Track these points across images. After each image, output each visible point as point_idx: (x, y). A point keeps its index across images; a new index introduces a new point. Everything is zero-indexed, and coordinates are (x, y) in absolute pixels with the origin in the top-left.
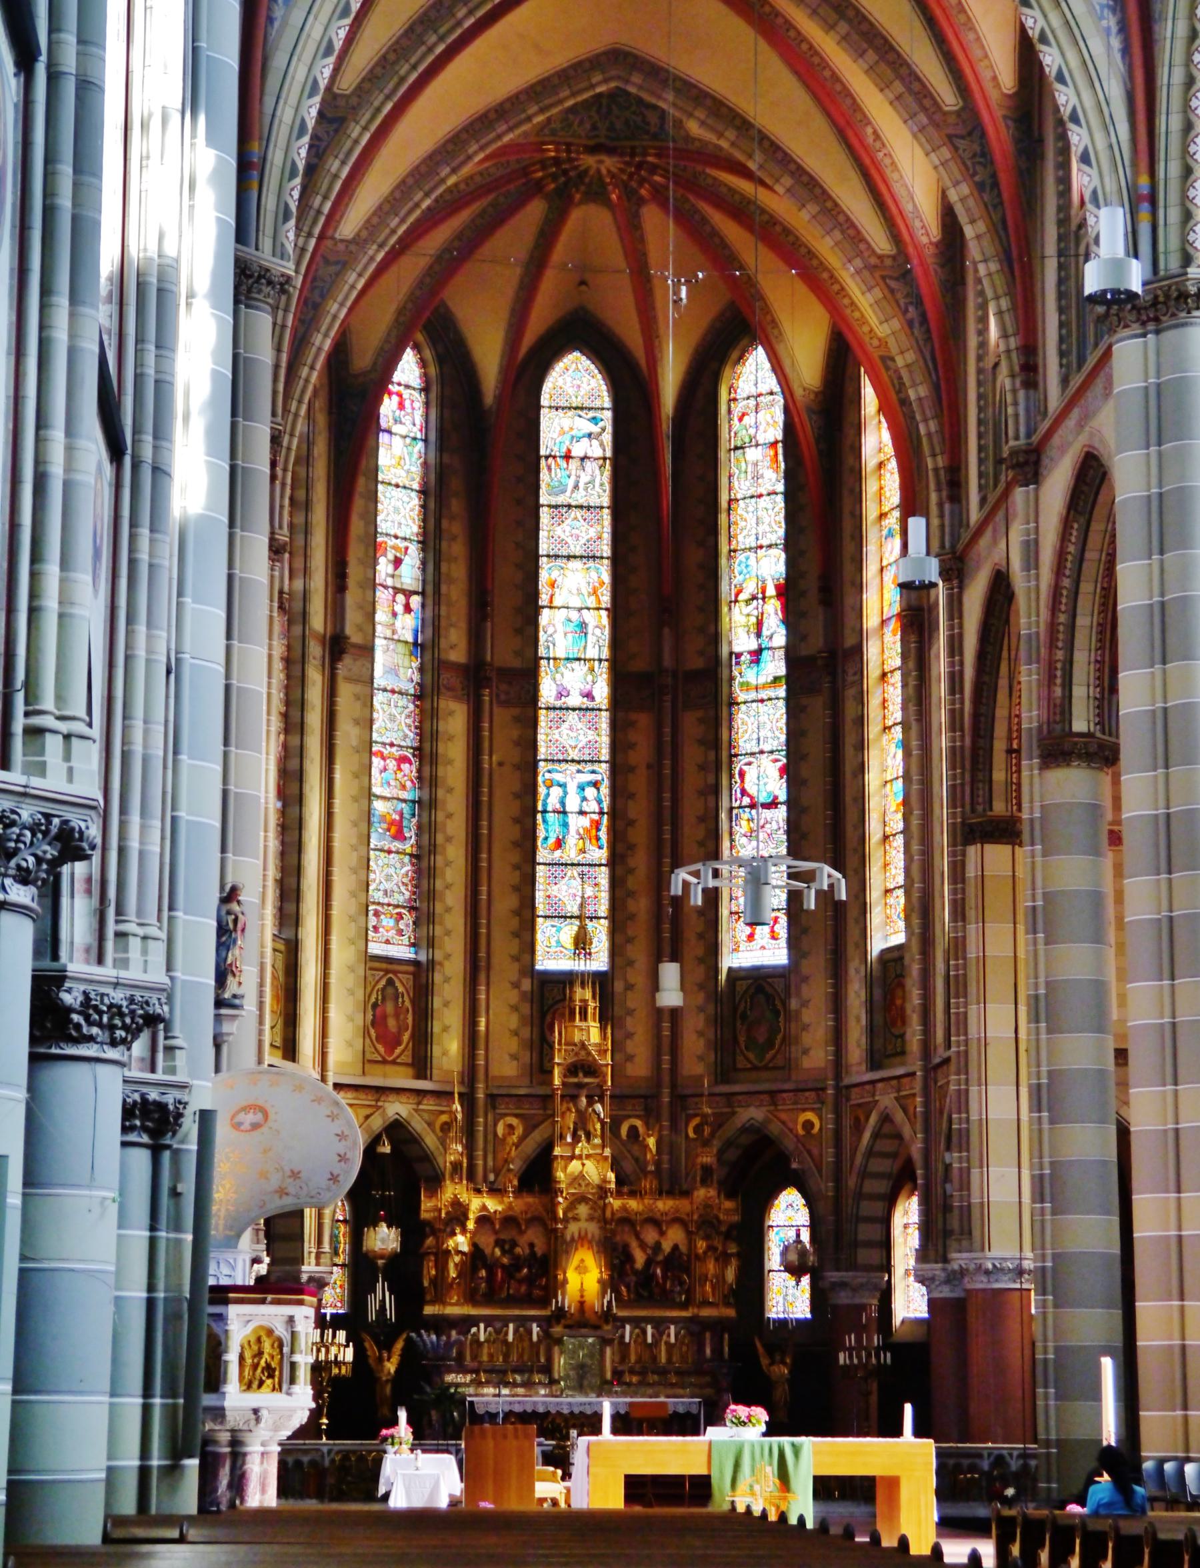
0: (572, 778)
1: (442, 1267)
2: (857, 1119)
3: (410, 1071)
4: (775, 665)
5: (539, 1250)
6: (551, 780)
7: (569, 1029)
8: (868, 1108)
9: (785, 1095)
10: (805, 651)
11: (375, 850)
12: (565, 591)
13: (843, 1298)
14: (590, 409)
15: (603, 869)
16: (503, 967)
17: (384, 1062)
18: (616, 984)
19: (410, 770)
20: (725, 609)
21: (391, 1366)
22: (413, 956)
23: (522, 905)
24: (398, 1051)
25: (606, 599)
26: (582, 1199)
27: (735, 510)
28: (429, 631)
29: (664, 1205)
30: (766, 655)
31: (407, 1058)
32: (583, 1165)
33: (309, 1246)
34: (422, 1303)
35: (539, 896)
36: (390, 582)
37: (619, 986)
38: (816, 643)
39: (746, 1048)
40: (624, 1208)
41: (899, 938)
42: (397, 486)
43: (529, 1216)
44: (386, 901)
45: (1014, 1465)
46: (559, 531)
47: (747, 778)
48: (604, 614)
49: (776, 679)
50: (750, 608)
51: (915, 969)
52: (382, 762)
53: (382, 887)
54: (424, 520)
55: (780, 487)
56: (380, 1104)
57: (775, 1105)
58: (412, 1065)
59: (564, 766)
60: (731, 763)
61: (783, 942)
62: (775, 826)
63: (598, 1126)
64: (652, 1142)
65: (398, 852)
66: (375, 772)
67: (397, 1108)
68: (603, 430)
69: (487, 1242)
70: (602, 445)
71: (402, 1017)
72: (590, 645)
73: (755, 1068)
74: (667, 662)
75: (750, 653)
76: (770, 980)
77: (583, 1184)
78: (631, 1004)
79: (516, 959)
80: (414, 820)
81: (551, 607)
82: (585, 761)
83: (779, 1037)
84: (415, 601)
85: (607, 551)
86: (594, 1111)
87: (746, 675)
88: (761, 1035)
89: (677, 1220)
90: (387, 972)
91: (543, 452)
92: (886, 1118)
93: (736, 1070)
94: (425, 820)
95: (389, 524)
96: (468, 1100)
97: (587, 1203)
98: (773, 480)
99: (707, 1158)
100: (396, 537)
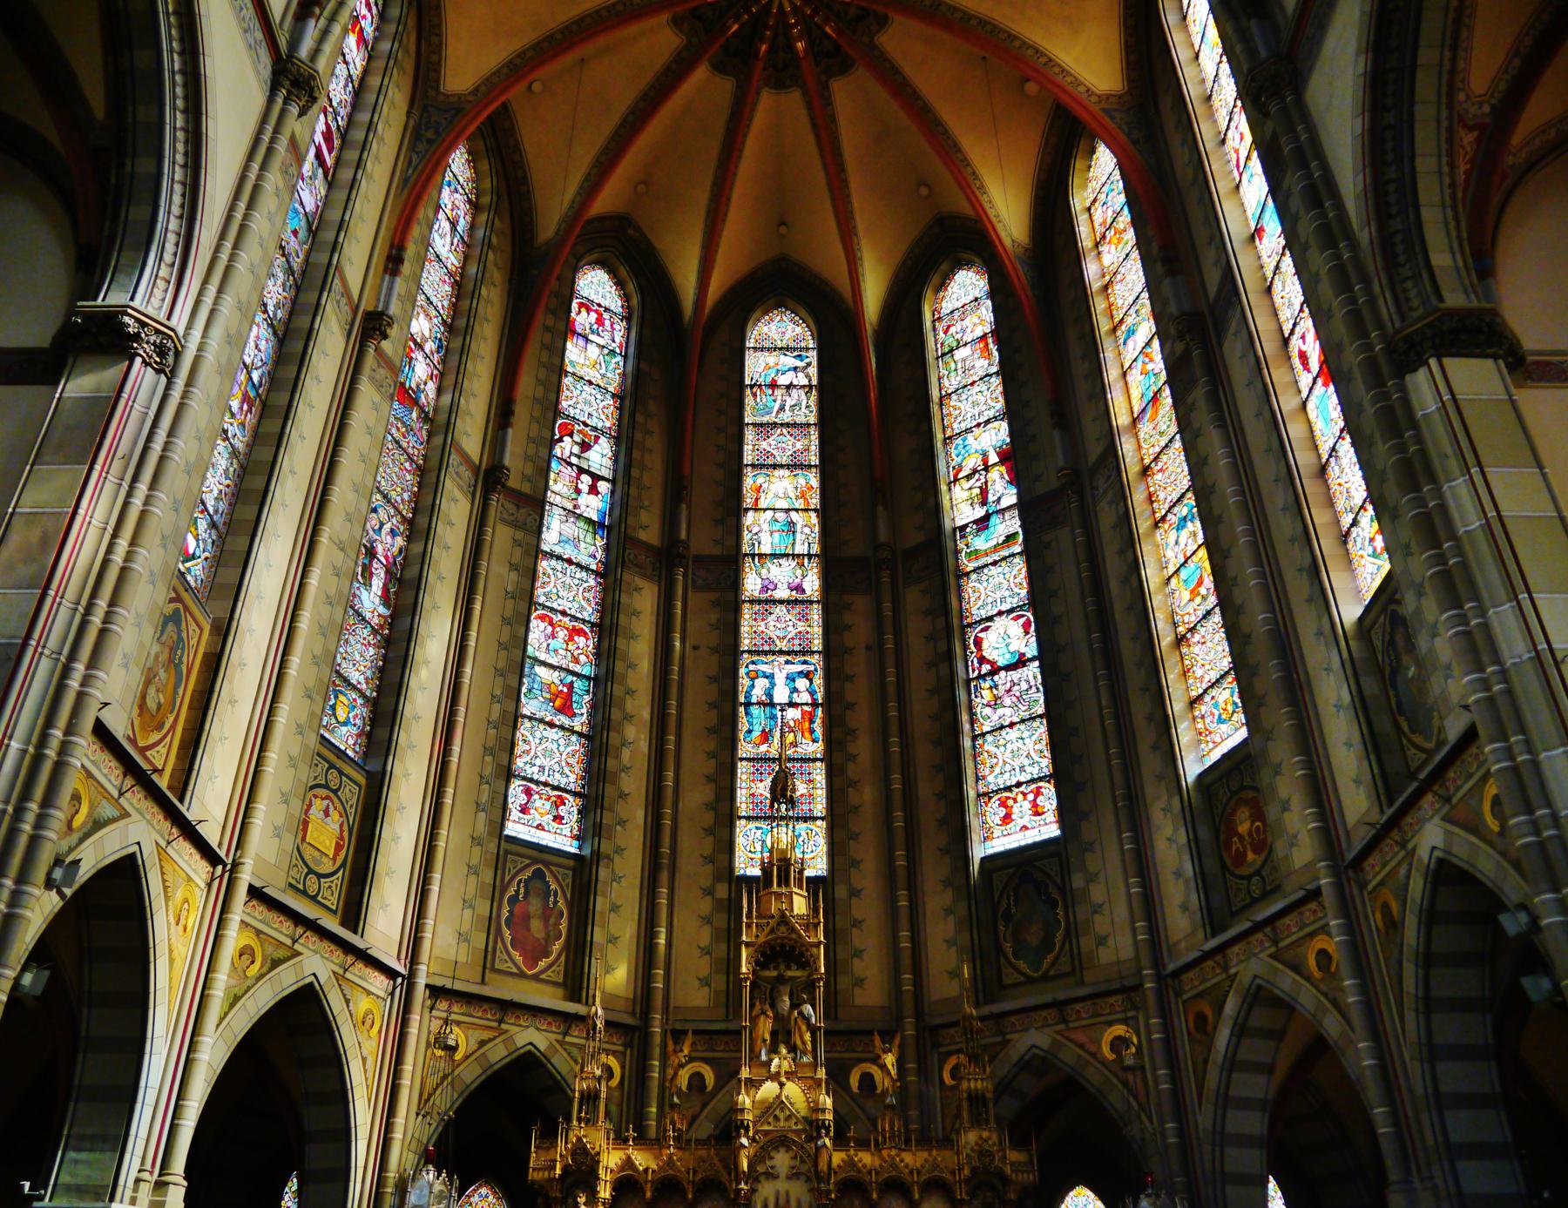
0: (781, 670)
2: (1201, 1018)
3: (560, 992)
6: (756, 672)
7: (763, 899)
9: (1078, 1006)
11: (530, 719)
12: (770, 495)
14: (795, 349)
15: (818, 764)
17: (522, 975)
18: (837, 888)
20: (944, 488)
22: (577, 851)
23: (718, 798)
24: (542, 964)
25: (815, 501)
26: (781, 1141)
27: (948, 404)
28: (617, 512)
29: (912, 1159)
30: (994, 520)
32: (782, 1085)
35: (741, 795)
36: (574, 460)
37: (841, 892)
38: (1056, 459)
40: (850, 1163)
42: (590, 383)
43: (699, 1177)
44: (543, 779)
46: (764, 445)
47: (985, 645)
48: (813, 515)
49: (1010, 538)
50: (973, 480)
52: (550, 629)
53: (538, 762)
54: (619, 420)
57: (1066, 1022)
58: (564, 985)
59: (771, 658)
60: (964, 634)
61: (1051, 817)
62: (1024, 686)
63: (808, 1036)
65: (562, 727)
67: (531, 1036)
68: (809, 365)
70: (807, 376)
71: (552, 920)
72: (798, 542)
73: (1030, 981)
74: (883, 535)
75: (975, 522)
76: (1038, 864)
77: (782, 1116)
78: (857, 913)
79: (709, 860)
80: (587, 698)
81: (756, 510)
82: (796, 653)
83: (1059, 935)
84: (603, 487)
85: (815, 460)
86: (801, 1013)
88: (1033, 937)
90: (535, 861)
91: (747, 382)
94: (600, 695)
95: (578, 411)
97: (788, 1149)
100: (586, 425)
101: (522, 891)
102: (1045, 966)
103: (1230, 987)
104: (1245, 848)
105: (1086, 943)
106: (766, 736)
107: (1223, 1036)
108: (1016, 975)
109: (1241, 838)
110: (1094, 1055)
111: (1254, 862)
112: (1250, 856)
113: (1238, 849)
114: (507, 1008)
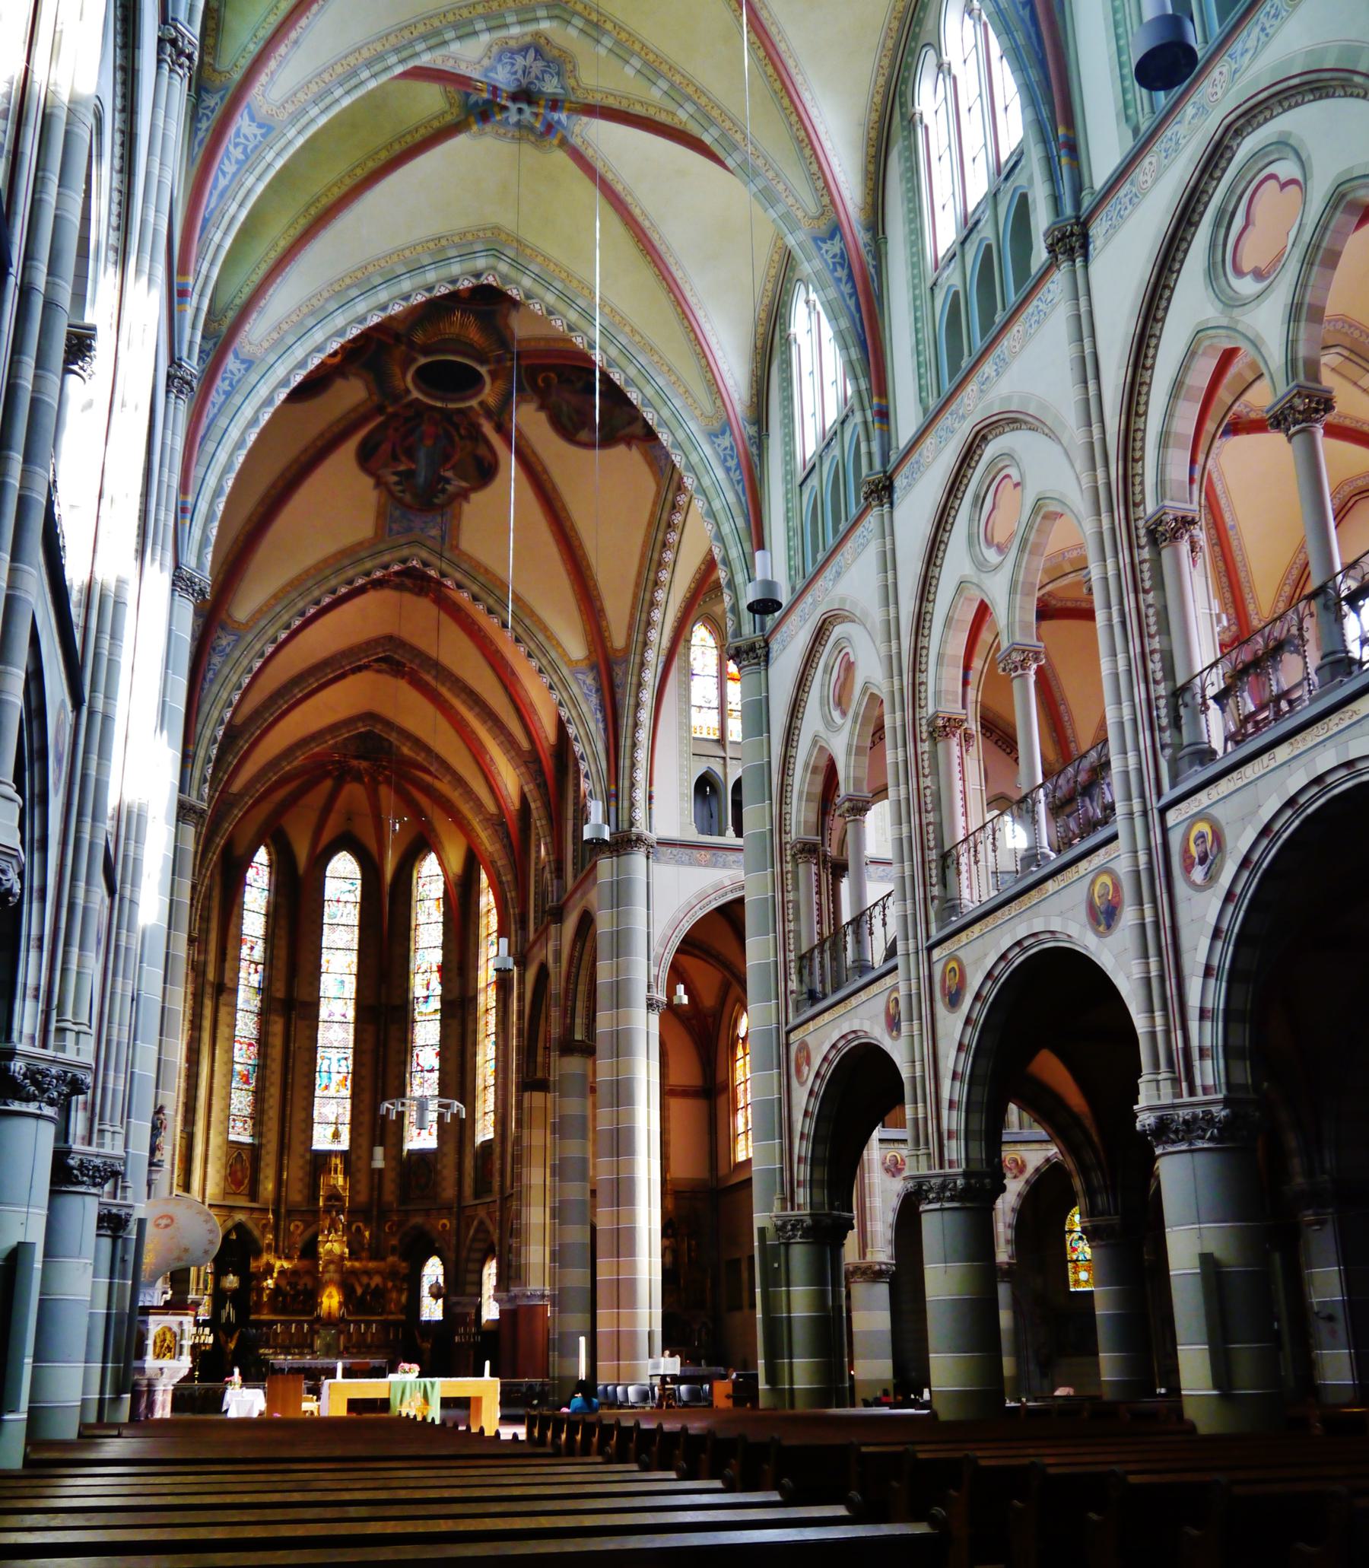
0: (334, 1055)
1: (260, 1296)
4: (435, 1004)
5: (309, 1287)
8: (472, 1218)
10: (450, 997)
13: (458, 1310)
16: (297, 1148)
19: (254, 1050)
21: (232, 1346)
25: (354, 969)
29: (372, 1265)
31: (246, 1192)
33: (193, 1285)
34: (250, 1313)
37: (353, 1157)
38: (455, 994)
41: (490, 1136)
45: (538, 1389)
51: (497, 1150)
55: (441, 919)
64: (367, 1234)
66: (236, 1050)
67: (240, 1217)
69: (283, 1283)
87: (420, 1008)
89: (378, 1272)
92: (481, 1223)
96: (276, 1213)
98: (438, 916)
99: (394, 1242)
106: (327, 1087)
107: (472, 1232)
114: (232, 1208)
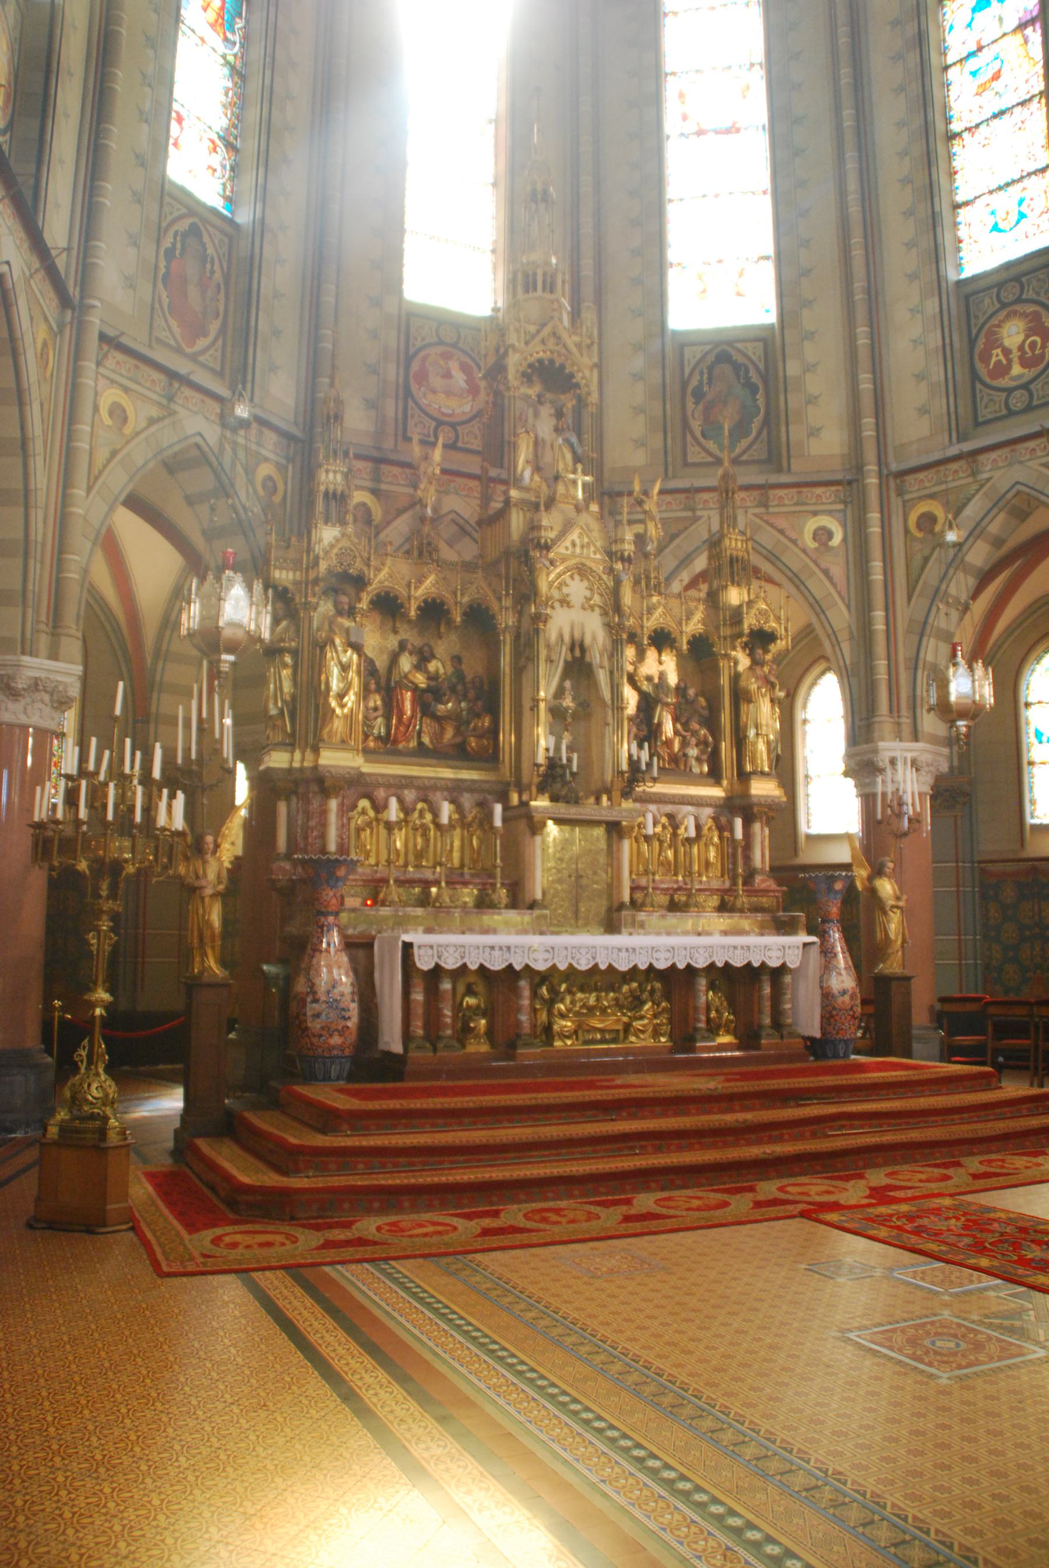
9: (781, 492)
39: (704, 435)
56: (173, 406)
57: (766, 506)
93: (686, 464)
101: (179, 246)
102: (738, 451)
103: (978, 491)
104: (1010, 362)
105: (796, 433)
108: (703, 454)
109: (1007, 352)
110: (794, 542)
111: (1020, 376)
112: (1016, 370)
113: (999, 362)
